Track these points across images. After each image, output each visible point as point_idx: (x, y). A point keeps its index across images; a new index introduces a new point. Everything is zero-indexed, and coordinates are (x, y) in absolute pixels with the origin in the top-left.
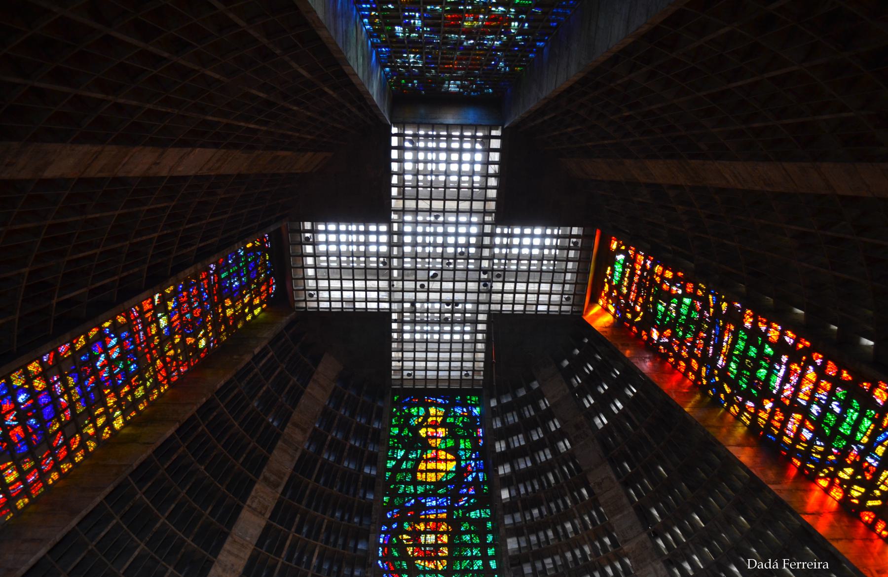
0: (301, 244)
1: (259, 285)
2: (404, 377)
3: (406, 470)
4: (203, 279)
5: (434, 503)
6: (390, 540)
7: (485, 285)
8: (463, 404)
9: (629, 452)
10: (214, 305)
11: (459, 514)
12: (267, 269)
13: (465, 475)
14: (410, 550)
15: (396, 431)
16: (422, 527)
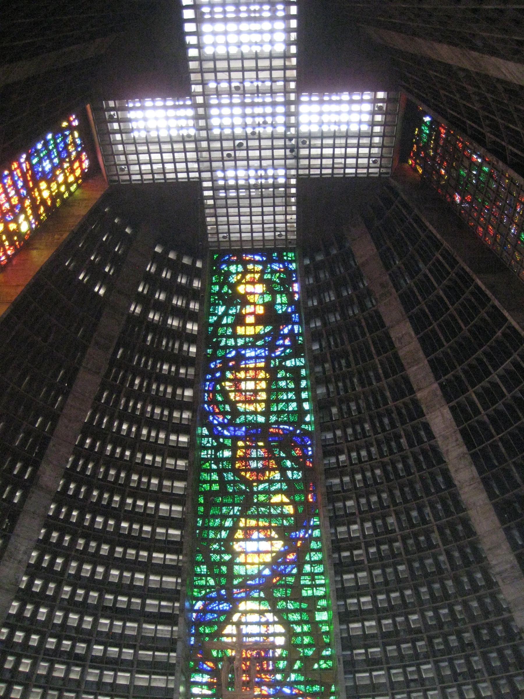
0: (105, 122)
1: (72, 163)
2: (221, 239)
3: (227, 325)
4: (16, 169)
5: (253, 354)
6: (214, 387)
7: (292, 151)
8: (280, 260)
9: (427, 310)
10: (30, 191)
11: (275, 363)
12: (76, 146)
13: (281, 327)
14: (232, 395)
15: (216, 288)
16: (242, 375)
